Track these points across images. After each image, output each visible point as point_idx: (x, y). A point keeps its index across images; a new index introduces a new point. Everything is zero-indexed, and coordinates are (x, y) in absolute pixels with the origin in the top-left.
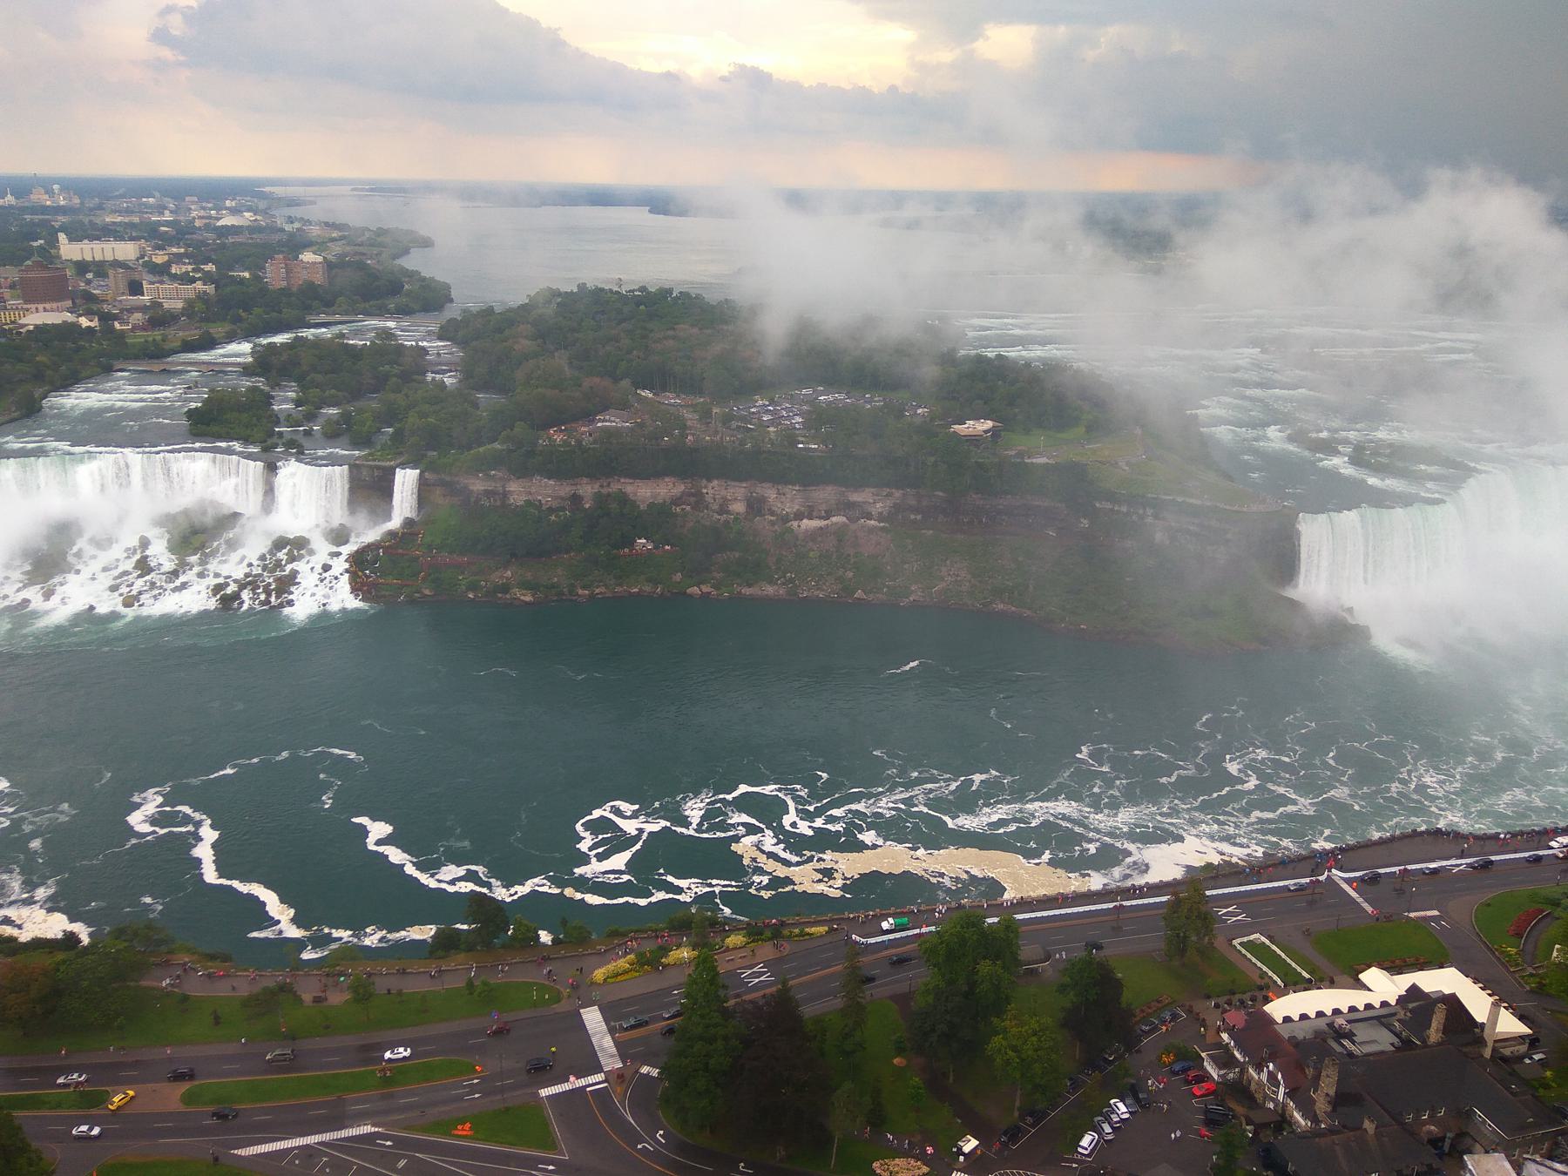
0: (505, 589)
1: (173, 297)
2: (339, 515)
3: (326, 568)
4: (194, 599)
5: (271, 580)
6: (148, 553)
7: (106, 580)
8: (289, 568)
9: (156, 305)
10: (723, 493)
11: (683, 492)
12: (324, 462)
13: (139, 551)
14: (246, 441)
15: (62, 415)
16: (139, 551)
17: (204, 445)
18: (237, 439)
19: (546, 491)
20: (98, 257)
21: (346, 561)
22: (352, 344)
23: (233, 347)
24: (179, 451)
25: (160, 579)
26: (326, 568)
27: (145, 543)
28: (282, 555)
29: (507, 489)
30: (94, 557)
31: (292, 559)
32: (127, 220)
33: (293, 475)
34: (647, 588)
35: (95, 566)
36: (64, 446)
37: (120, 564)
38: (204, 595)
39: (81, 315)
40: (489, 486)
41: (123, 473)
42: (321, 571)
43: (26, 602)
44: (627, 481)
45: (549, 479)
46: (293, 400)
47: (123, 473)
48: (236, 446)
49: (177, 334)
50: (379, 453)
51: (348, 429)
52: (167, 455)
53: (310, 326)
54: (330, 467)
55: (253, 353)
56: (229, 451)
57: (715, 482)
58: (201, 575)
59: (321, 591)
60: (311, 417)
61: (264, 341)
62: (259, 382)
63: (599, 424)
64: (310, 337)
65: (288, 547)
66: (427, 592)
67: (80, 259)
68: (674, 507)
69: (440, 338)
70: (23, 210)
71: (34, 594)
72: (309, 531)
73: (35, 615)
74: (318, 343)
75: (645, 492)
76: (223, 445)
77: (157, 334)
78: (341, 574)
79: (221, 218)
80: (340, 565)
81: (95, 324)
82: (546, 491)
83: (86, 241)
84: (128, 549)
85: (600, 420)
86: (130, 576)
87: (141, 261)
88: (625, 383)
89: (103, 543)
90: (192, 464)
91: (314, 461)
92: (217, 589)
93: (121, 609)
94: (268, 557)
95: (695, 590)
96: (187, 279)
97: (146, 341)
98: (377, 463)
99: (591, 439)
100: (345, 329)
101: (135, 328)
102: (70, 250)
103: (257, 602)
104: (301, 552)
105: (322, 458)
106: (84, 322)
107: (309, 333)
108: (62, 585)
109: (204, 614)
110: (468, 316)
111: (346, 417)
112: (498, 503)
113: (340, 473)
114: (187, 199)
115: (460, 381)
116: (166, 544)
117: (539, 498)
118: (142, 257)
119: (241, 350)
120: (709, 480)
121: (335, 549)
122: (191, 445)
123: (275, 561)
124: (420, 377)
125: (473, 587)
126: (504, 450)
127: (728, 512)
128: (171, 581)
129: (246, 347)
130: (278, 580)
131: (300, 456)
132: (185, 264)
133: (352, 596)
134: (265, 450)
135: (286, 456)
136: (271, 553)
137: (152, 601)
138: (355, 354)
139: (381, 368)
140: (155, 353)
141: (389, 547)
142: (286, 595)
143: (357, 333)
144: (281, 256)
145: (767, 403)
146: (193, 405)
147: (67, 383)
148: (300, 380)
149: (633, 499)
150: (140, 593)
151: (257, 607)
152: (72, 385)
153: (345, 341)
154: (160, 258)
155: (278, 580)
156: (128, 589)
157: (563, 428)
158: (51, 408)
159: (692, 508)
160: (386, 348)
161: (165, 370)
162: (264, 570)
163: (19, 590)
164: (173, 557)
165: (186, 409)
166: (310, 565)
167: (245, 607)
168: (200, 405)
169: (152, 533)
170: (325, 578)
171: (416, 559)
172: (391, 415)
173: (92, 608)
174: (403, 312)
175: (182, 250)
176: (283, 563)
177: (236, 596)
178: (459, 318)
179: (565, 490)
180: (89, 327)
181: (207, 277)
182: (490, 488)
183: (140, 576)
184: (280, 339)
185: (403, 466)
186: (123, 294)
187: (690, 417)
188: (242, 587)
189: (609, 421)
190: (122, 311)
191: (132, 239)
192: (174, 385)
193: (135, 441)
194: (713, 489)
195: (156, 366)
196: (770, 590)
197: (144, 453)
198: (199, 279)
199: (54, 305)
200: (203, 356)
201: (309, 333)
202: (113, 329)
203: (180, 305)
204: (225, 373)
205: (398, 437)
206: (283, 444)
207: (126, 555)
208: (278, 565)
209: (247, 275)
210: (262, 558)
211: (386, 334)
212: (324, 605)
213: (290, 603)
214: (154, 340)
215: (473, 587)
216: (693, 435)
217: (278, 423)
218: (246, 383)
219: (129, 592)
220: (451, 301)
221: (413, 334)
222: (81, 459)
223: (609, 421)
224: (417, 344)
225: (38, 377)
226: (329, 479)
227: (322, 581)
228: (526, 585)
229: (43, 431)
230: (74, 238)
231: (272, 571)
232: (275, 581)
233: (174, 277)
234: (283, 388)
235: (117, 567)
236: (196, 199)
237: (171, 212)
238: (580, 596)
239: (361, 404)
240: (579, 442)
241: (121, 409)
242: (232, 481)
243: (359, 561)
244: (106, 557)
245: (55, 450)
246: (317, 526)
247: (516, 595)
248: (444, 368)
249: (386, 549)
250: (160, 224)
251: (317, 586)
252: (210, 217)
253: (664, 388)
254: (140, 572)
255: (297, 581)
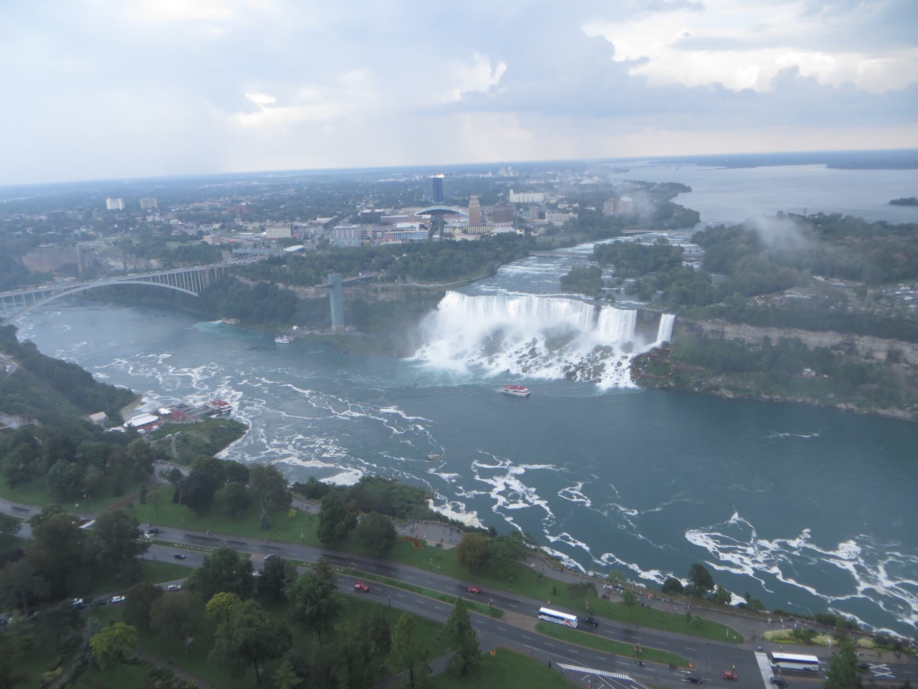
0: (717, 388)
1: (557, 220)
2: (629, 336)
3: (619, 364)
4: (553, 372)
5: (591, 367)
6: (536, 346)
7: (516, 358)
8: (601, 362)
9: (550, 224)
10: (870, 345)
11: (840, 344)
12: (625, 307)
13: (532, 346)
14: (587, 293)
15: (506, 277)
16: (532, 346)
17: (567, 295)
18: (583, 293)
19: (749, 334)
20: (526, 201)
21: (630, 361)
22: (644, 245)
23: (584, 246)
24: (555, 297)
25: (540, 361)
26: (619, 364)
27: (535, 341)
28: (598, 355)
29: (725, 330)
30: (512, 346)
31: (603, 357)
32: (539, 182)
33: (609, 313)
34: (809, 400)
35: (512, 350)
36: (504, 291)
37: (523, 351)
38: (559, 370)
39: (516, 229)
40: (714, 327)
41: (529, 306)
42: (616, 366)
43: (481, 364)
44: (803, 331)
45: (752, 325)
46: (611, 274)
47: (529, 306)
48: (583, 296)
49: (558, 239)
50: (653, 305)
51: (639, 291)
52: (550, 299)
53: (623, 235)
54: (627, 311)
55: (595, 249)
56: (579, 299)
57: (865, 338)
58: (559, 361)
59: (616, 376)
60: (619, 283)
61: (601, 243)
62: (596, 263)
63: (787, 296)
64: (623, 241)
65: (601, 351)
66: (672, 384)
67: (518, 202)
68: (833, 351)
69: (692, 241)
70: (496, 179)
71: (484, 360)
72: (613, 343)
73: (485, 371)
74: (627, 244)
75: (813, 340)
76: (576, 295)
77: (549, 238)
78: (627, 369)
79: (582, 180)
80: (626, 364)
81: (523, 233)
82: (749, 334)
83: (521, 193)
84: (527, 344)
85: (787, 293)
86: (527, 357)
87: (544, 202)
88: (806, 272)
89: (517, 339)
90: (561, 304)
91: (619, 307)
92: (566, 368)
93: (521, 373)
94: (592, 355)
95: (842, 406)
96: (565, 211)
97: (545, 242)
98: (652, 310)
99: (781, 304)
100: (640, 237)
101: (540, 235)
102: (514, 198)
103: (583, 378)
104: (608, 354)
105: (624, 305)
106: (518, 232)
107: (622, 239)
108: (497, 357)
109: (558, 380)
110: (709, 230)
111: (638, 285)
112: (718, 337)
113: (632, 314)
114: (567, 171)
115: (701, 267)
116: (544, 343)
117: (744, 337)
118: (545, 200)
119: (588, 247)
120: (861, 334)
121: (624, 354)
122: (561, 294)
123: (595, 357)
124: (678, 264)
125: (698, 385)
126: (725, 307)
127: (873, 358)
128: (544, 362)
129: (591, 246)
130: (595, 368)
131: (613, 303)
132: (565, 203)
133: (631, 381)
134: (597, 299)
135: (606, 303)
136: (593, 353)
137: (535, 371)
138: (646, 250)
139: (658, 258)
140: (548, 247)
141: (654, 357)
142: (598, 376)
143: (647, 239)
144: (612, 199)
145: (908, 288)
146: (564, 274)
147: (509, 261)
148: (617, 265)
149: (805, 343)
150: (530, 366)
151: (583, 380)
152: (509, 262)
153: (641, 243)
154: (553, 201)
155: (595, 368)
156: (525, 363)
157: (763, 296)
158: (501, 273)
159: (846, 353)
160: (663, 248)
161: (551, 256)
162: (588, 362)
163: (479, 358)
164: (547, 350)
165: (561, 276)
166: (611, 362)
167: (578, 380)
168: (567, 274)
169: (538, 337)
170: (618, 370)
171: (667, 365)
172: (661, 285)
173: (508, 371)
174: (673, 227)
175: (564, 197)
176: (598, 359)
177: (574, 373)
178: (704, 231)
179: (761, 333)
180: (520, 235)
181: (575, 210)
182: (714, 329)
183: (531, 358)
184: (608, 241)
185: (666, 312)
186: (536, 218)
187: (851, 295)
188: (577, 369)
189: (793, 294)
190: (535, 226)
191: (541, 192)
192: (555, 264)
193: (535, 291)
194: (864, 343)
195: (548, 254)
196: (899, 413)
197: (539, 297)
198: (571, 211)
199: (506, 224)
200: (570, 250)
201: (622, 239)
202: (529, 236)
203: (561, 224)
204: (580, 259)
205: (665, 297)
206: (605, 296)
207: (526, 347)
208: (596, 360)
209: (593, 209)
210: (588, 355)
211: (663, 240)
212: (616, 384)
213: (600, 381)
214: (548, 241)
215: (698, 385)
216: (852, 306)
217: (603, 285)
218: (589, 264)
219: (526, 365)
220: (699, 221)
221: (678, 239)
222: (511, 298)
223: (793, 294)
224: (679, 245)
225: (497, 258)
226: (626, 317)
227: (616, 371)
228: (730, 388)
229: (496, 283)
230: (515, 192)
231: (592, 362)
232: (593, 368)
233: (559, 210)
234: (607, 267)
235: (521, 352)
236: (571, 171)
237: (560, 178)
238: (763, 399)
239: (646, 277)
240: (773, 306)
241: (531, 274)
242: (579, 314)
243: (637, 363)
244: (517, 347)
245: (500, 293)
246: (617, 341)
247: (723, 392)
248: (693, 259)
249: (652, 358)
250: (553, 184)
251: (613, 373)
252: (578, 180)
253: (832, 275)
254: (531, 356)
255: (604, 369)
